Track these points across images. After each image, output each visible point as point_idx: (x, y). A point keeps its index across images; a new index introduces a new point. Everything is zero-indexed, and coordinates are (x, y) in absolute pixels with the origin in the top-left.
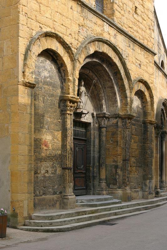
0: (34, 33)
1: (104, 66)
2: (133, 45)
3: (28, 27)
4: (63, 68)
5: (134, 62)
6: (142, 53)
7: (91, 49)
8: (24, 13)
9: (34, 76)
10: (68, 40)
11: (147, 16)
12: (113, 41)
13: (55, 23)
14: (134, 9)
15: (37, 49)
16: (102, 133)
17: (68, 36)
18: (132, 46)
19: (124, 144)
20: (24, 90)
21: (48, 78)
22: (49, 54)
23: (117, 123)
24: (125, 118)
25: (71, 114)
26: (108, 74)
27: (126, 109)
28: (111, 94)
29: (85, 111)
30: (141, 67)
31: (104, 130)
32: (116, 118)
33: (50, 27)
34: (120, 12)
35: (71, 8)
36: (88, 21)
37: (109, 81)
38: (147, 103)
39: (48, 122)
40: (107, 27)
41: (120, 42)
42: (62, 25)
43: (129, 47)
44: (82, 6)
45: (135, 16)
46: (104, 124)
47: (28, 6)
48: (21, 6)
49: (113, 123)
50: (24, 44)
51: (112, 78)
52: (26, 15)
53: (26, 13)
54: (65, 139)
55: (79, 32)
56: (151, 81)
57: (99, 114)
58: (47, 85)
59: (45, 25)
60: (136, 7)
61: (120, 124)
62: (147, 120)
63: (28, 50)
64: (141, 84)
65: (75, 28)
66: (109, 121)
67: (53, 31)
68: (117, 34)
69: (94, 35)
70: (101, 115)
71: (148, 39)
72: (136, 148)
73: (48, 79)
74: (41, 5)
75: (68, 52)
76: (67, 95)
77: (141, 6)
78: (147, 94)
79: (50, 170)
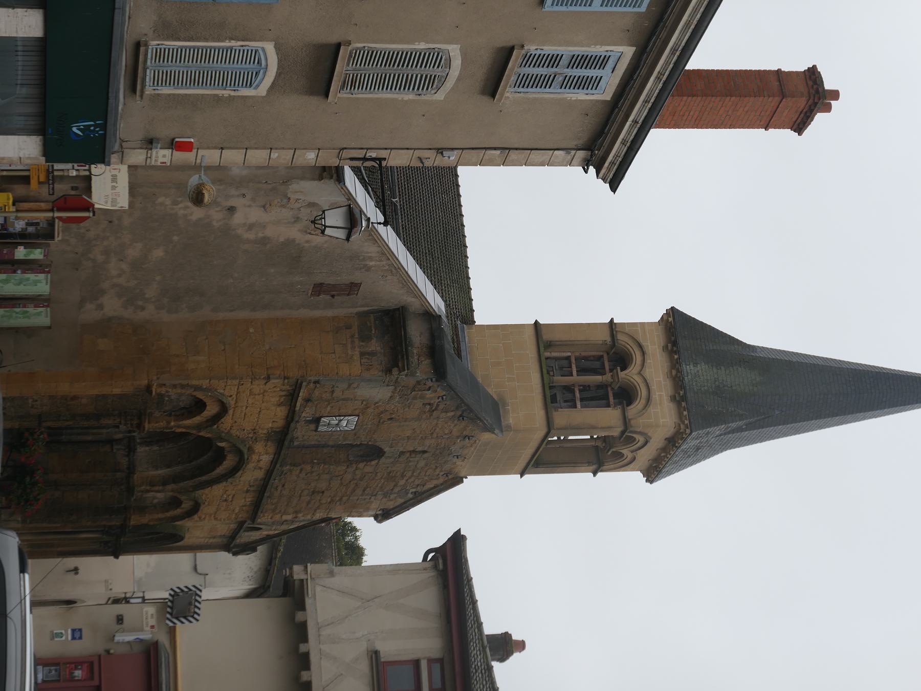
0: (222, 391)
11: (318, 508)
12: (251, 466)
15: (200, 395)
18: (252, 489)
22: (200, 406)
40: (266, 459)
45: (306, 492)
51: (194, 463)
61: (118, 475)
63: (198, 388)
64: (191, 503)
75: (207, 421)
78: (178, 511)
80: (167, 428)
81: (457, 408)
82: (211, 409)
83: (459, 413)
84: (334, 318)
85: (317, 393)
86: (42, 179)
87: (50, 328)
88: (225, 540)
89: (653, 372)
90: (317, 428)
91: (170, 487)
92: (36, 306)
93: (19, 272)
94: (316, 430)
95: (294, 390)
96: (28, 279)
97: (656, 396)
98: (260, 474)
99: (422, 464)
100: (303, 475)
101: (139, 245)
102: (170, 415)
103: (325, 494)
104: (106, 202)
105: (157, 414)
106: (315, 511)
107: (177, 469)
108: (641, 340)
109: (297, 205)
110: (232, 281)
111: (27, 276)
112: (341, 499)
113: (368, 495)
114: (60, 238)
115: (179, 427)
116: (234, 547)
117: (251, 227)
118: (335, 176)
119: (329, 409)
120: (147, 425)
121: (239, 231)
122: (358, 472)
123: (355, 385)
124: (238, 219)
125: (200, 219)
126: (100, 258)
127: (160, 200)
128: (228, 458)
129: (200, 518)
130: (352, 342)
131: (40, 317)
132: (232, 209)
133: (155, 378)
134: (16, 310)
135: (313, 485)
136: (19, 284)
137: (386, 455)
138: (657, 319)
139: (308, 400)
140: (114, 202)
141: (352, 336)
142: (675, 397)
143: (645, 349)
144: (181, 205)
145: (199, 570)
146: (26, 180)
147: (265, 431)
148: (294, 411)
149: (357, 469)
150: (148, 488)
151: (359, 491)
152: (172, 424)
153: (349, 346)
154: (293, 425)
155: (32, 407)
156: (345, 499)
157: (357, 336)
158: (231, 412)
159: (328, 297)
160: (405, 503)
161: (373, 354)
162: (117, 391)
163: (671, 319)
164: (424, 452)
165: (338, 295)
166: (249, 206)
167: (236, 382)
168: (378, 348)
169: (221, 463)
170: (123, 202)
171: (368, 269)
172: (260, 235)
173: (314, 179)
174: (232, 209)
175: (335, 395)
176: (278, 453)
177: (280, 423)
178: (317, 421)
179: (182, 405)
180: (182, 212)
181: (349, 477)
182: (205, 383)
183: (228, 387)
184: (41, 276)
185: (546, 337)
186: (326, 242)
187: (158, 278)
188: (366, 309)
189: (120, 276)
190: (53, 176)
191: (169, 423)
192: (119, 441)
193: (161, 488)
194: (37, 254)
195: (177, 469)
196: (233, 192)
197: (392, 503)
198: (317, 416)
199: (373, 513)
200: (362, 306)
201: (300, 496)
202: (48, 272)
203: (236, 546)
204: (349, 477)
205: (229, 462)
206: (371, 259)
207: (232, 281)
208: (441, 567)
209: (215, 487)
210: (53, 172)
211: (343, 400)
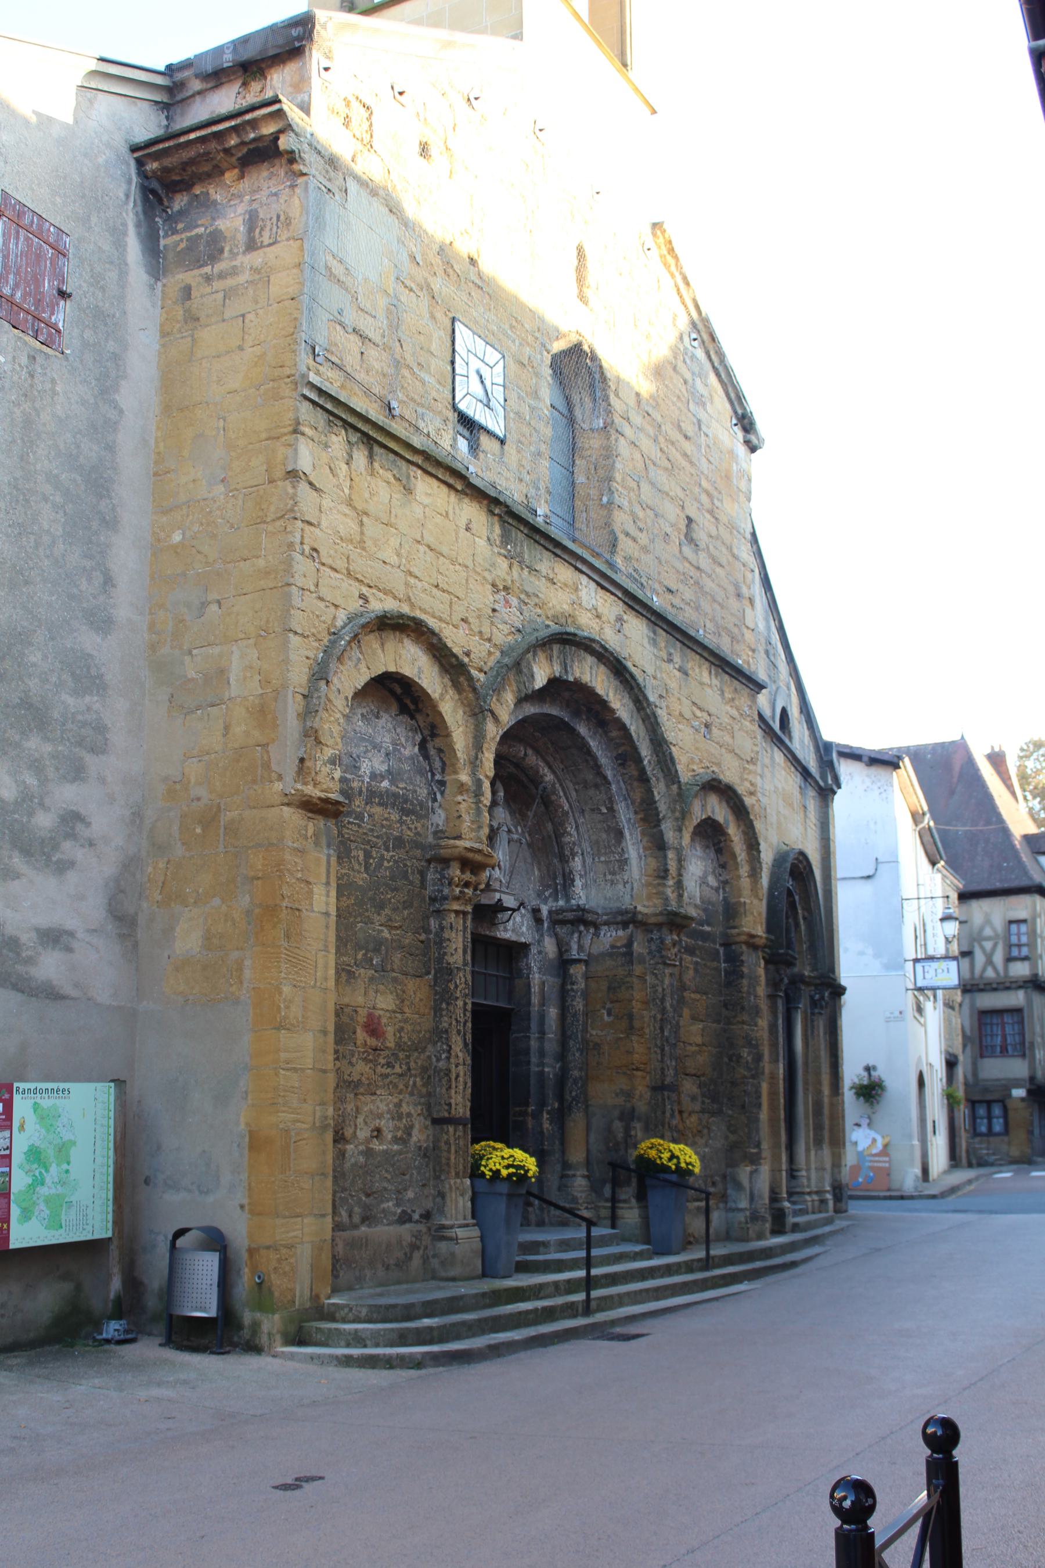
0: (342, 617)
1: (582, 730)
2: (683, 656)
3: (321, 599)
4: (438, 742)
5: (688, 714)
6: (715, 682)
7: (535, 669)
8: (307, 548)
9: (337, 774)
10: (456, 639)
11: (730, 549)
12: (611, 639)
13: (412, 581)
14: (682, 524)
15: (352, 676)
16: (573, 983)
17: (455, 627)
18: (677, 658)
19: (658, 1026)
20: (303, 823)
21: (383, 777)
22: (394, 692)
23: (629, 944)
24: (659, 926)
25: (465, 913)
26: (595, 759)
27: (663, 893)
28: (604, 836)
29: (509, 901)
30: (710, 732)
31: (577, 971)
32: (625, 925)
33: (395, 597)
34: (634, 540)
35: (468, 529)
36: (526, 571)
37: (596, 786)
38: (737, 869)
39: (381, 944)
40: (590, 594)
41: (635, 643)
42: (437, 586)
43: (670, 661)
44: (506, 518)
45: (687, 550)
46: (581, 948)
47: (324, 523)
48: (299, 523)
49: (613, 947)
50: (307, 658)
51: (609, 774)
52: (315, 555)
53: (315, 550)
54: (444, 1006)
55: (494, 610)
56: (747, 784)
57: (561, 911)
58: (380, 804)
59: (379, 590)
60: (690, 520)
62: (739, 934)
63: (320, 674)
65: (483, 597)
66: (597, 935)
67: (406, 609)
68: (625, 617)
69: (547, 622)
70: (570, 916)
71: (736, 630)
72: (699, 1040)
73: (385, 784)
74: (365, 519)
75: (456, 686)
76: (452, 842)
77: (708, 516)
78: (734, 831)
79: (386, 1125)
80: (478, 794)
82: (411, 661)
87: (119, 1083)
88: (811, 793)
91: (670, 836)
95: (347, 425)
98: (637, 628)
100: (643, 538)
102: (442, 783)
103: (692, 515)
105: (439, 818)
106: (735, 557)
107: (624, 814)
112: (709, 494)
115: (475, 763)
116: (825, 781)
122: (637, 419)
123: (338, 270)
128: (586, 678)
129: (752, 794)
130: (222, 276)
133: (278, 786)
141: (208, 279)
145: (871, 873)
147: (504, 564)
149: (628, 420)
150: (671, 883)
151: (687, 446)
152: (464, 777)
153: (230, 282)
155: (403, 1141)
156: (704, 484)
157: (208, 269)
160: (718, 375)
161: (252, 221)
167: (302, 566)
169: (603, 704)
175: (376, 337)
177: (471, 511)
178: (467, 423)
179: (410, 750)
181: (645, 444)
183: (324, 591)
191: (461, 787)
192: (562, 947)
193: (671, 855)
195: (624, 814)
197: (716, 399)
198: (453, 417)
199: (741, 450)
200: (120, 245)
201: (698, 568)
203: (824, 777)
209: (670, 736)
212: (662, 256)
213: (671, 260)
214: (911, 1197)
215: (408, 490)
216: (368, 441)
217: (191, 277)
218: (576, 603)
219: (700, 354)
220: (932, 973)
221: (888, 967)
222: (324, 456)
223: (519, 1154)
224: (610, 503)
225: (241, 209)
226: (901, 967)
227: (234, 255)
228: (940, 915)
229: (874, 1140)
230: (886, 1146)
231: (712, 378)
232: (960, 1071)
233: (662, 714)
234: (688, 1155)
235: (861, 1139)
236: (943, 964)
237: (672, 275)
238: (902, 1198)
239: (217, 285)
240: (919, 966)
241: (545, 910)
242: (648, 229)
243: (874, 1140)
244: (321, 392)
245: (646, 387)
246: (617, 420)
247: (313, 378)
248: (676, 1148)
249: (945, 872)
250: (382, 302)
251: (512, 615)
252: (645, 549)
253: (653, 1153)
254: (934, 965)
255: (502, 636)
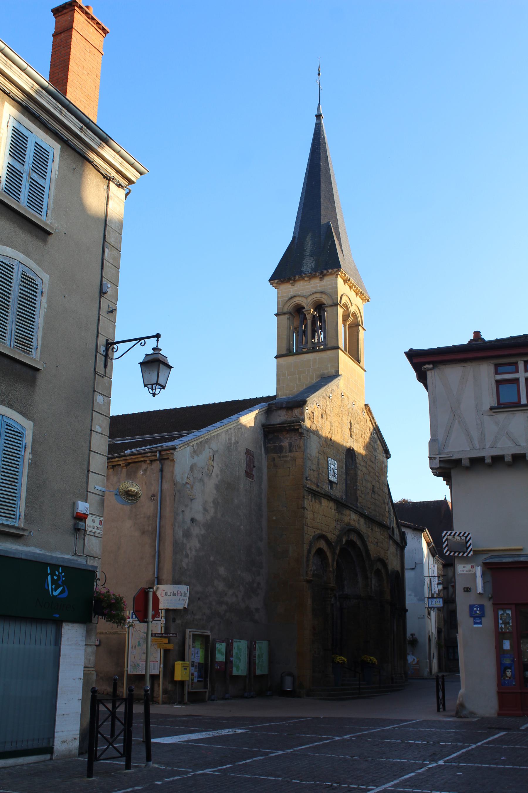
0: (311, 537)
10: (330, 536)
11: (382, 490)
12: (357, 525)
15: (313, 551)
22: (320, 551)
41: (361, 525)
43: (369, 528)
45: (373, 495)
63: (309, 551)
78: (383, 571)
81: (325, 398)
82: (322, 544)
83: (328, 398)
84: (268, 468)
85: (314, 480)
86: (166, 641)
88: (399, 549)
89: (305, 289)
90: (335, 483)
92: (255, 649)
93: (231, 659)
94: (337, 484)
95: (312, 493)
96: (237, 654)
97: (320, 289)
98: (362, 521)
99: (357, 426)
100: (363, 496)
101: (216, 582)
104: (184, 600)
106: (383, 492)
108: (288, 298)
109: (191, 478)
110: (242, 527)
111: (234, 654)
112: (378, 477)
113: (375, 460)
114: (209, 632)
115: (333, 565)
116: (402, 544)
117: (205, 510)
118: (171, 451)
119: (323, 474)
120: (332, 585)
121: (208, 517)
122: (362, 463)
123: (309, 456)
124: (199, 517)
125: (199, 541)
126: (224, 607)
127: (184, 565)
130: (283, 457)
131: (262, 647)
132: (193, 520)
134: (257, 661)
135: (369, 491)
136: (240, 659)
137: (352, 446)
138: (275, 291)
139: (318, 486)
140: (184, 595)
141: (279, 457)
142: (320, 278)
143: (293, 295)
144: (189, 552)
146: (167, 652)
148: (325, 495)
149: (360, 464)
151: (373, 465)
152: (331, 569)
153: (285, 459)
154: (333, 497)
156: (377, 474)
157: (279, 454)
158: (325, 533)
159: (255, 469)
160: (380, 440)
161: (290, 445)
162: (310, 601)
163: (276, 281)
164: (350, 423)
165: (253, 463)
166: (191, 509)
167: (306, 528)
168: (287, 441)
169: (355, 543)
170: (184, 589)
171: (237, 442)
172: (212, 505)
173: (174, 466)
174: (193, 520)
175: (315, 469)
176: (350, 508)
177: (331, 504)
178: (331, 482)
180: (194, 553)
181: (364, 469)
182: (306, 547)
184: (235, 645)
185: (285, 352)
186: (218, 465)
187: (239, 573)
188: (263, 448)
189: (236, 596)
190: (165, 634)
194: (221, 647)
196: (180, 517)
198: (328, 482)
199: (385, 459)
201: (375, 499)
202: (232, 640)
203: (402, 543)
204: (364, 469)
205: (354, 537)
206: (230, 439)
207: (242, 527)
208: (431, 366)
209: (369, 548)
210: (162, 634)
211: (318, 464)
212: (367, 413)
213: (369, 413)
214: (426, 679)
215: (321, 503)
216: (315, 495)
217: (275, 455)
218: (350, 519)
219: (376, 436)
220: (434, 602)
221: (419, 600)
222: (308, 502)
223: (343, 658)
224: (356, 489)
225: (287, 441)
226: (424, 600)
227: (286, 452)
228: (437, 582)
229: (414, 659)
230: (418, 661)
231: (379, 442)
232: (443, 635)
233: (367, 542)
234: (374, 660)
235: (410, 659)
236: (438, 600)
237: (369, 417)
238: (423, 679)
239: (282, 459)
240: (429, 600)
241: (337, 595)
242: (364, 407)
243: (414, 659)
244: (308, 488)
245: (364, 452)
246: (358, 465)
247: (308, 486)
248: (372, 658)
249: (438, 559)
250: (316, 459)
251: (339, 527)
252: (364, 499)
253: (365, 659)
254: (435, 600)
255: (337, 532)
